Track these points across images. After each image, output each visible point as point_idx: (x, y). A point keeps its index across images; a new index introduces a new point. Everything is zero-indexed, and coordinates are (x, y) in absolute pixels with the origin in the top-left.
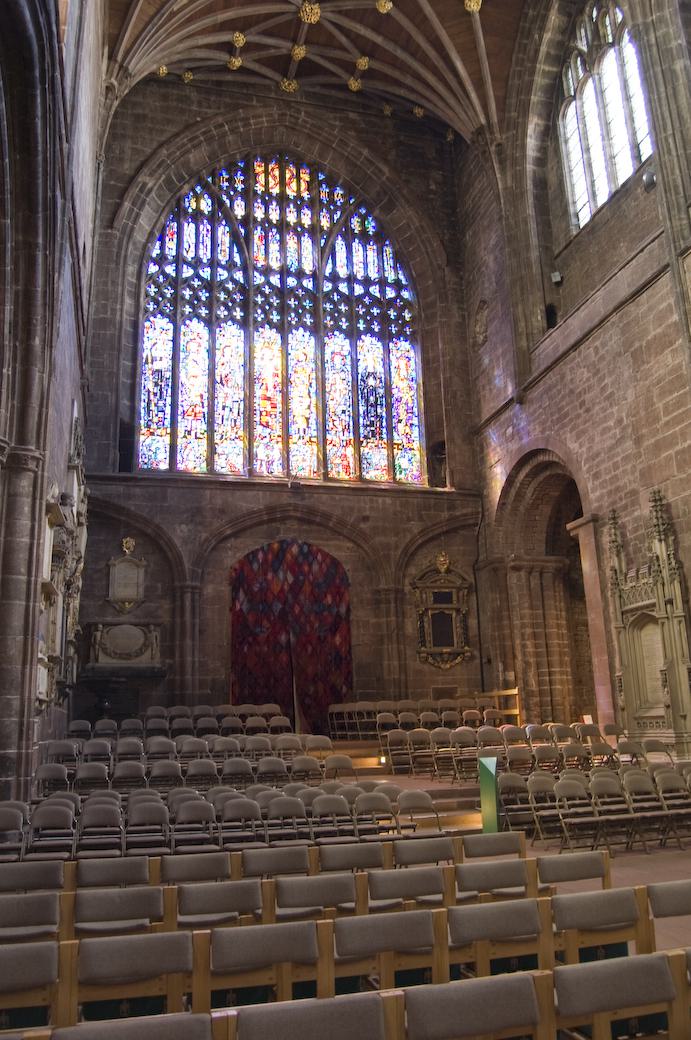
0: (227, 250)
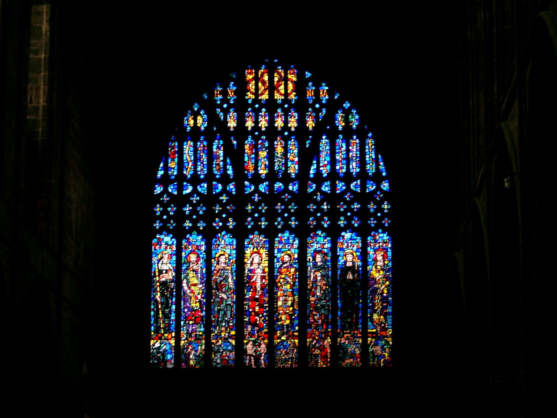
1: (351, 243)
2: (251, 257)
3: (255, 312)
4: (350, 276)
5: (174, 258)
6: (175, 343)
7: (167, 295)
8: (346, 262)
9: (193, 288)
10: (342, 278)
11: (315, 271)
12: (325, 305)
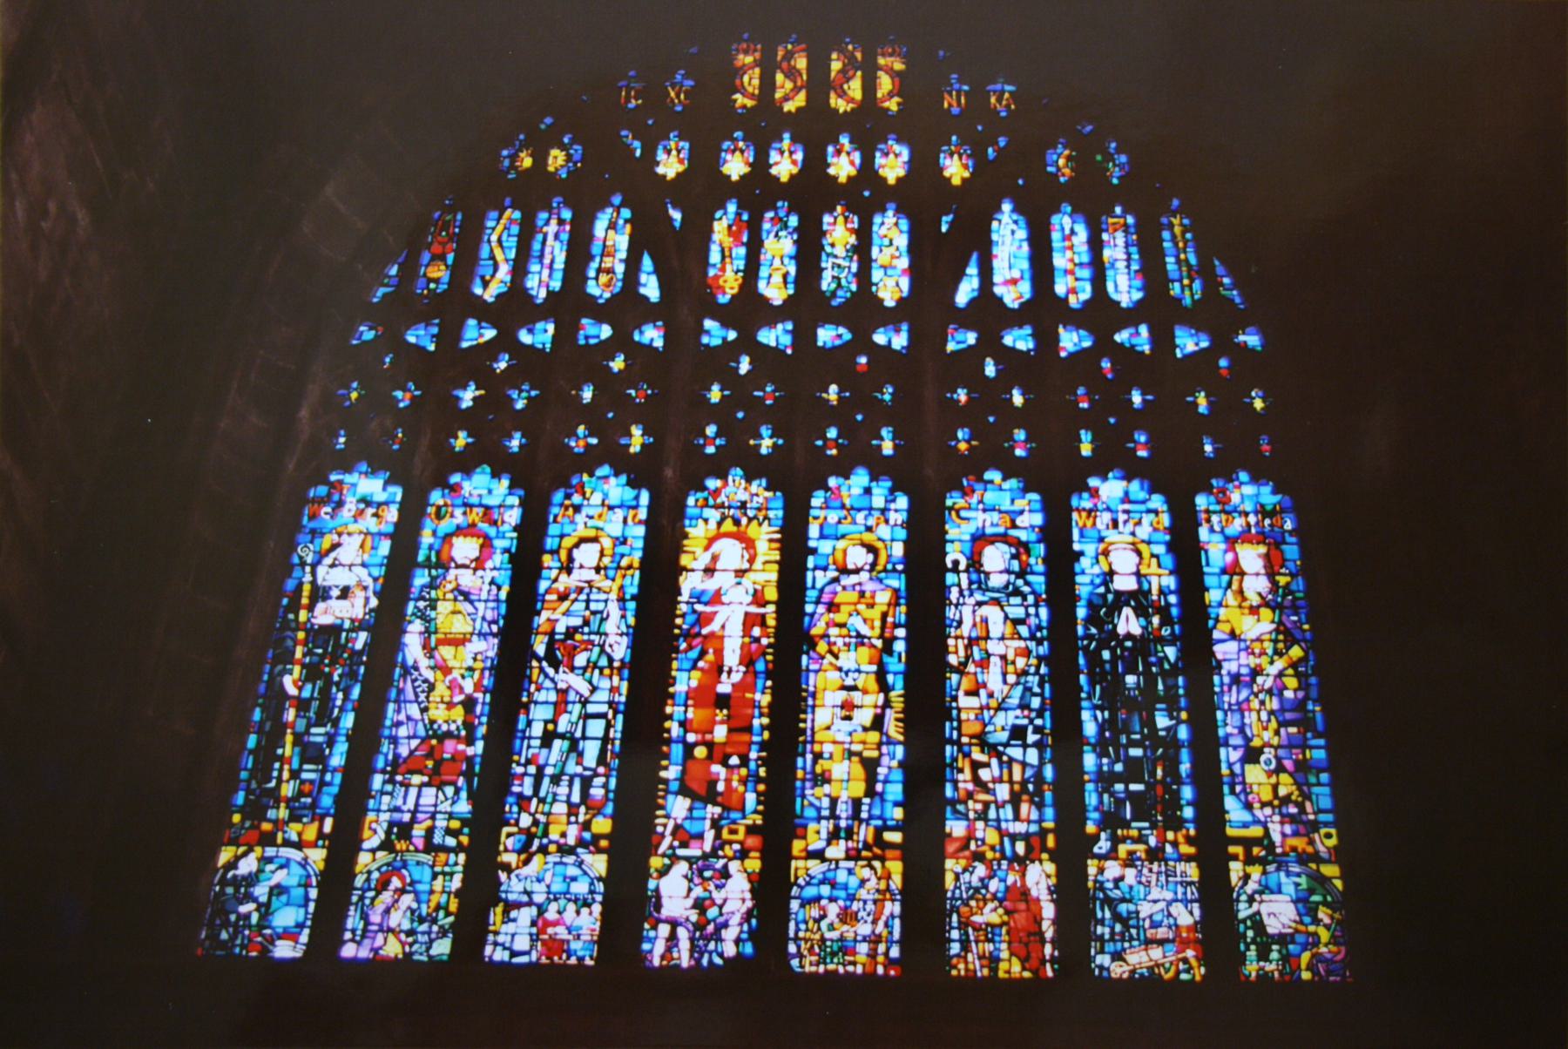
0: (620, 269)
1: (1127, 512)
2: (707, 548)
3: (710, 745)
4: (1128, 623)
5: (385, 547)
6: (327, 860)
7: (331, 675)
8: (1110, 574)
9: (446, 652)
10: (1093, 631)
11: (980, 604)
12: (1024, 728)
